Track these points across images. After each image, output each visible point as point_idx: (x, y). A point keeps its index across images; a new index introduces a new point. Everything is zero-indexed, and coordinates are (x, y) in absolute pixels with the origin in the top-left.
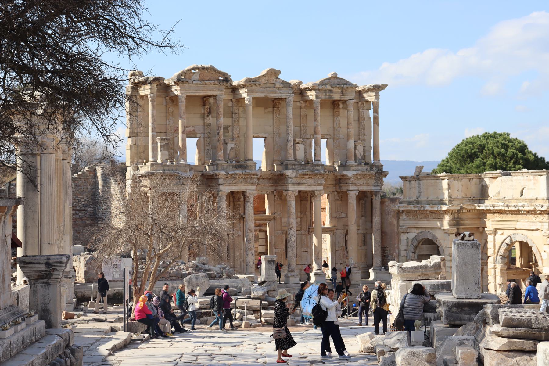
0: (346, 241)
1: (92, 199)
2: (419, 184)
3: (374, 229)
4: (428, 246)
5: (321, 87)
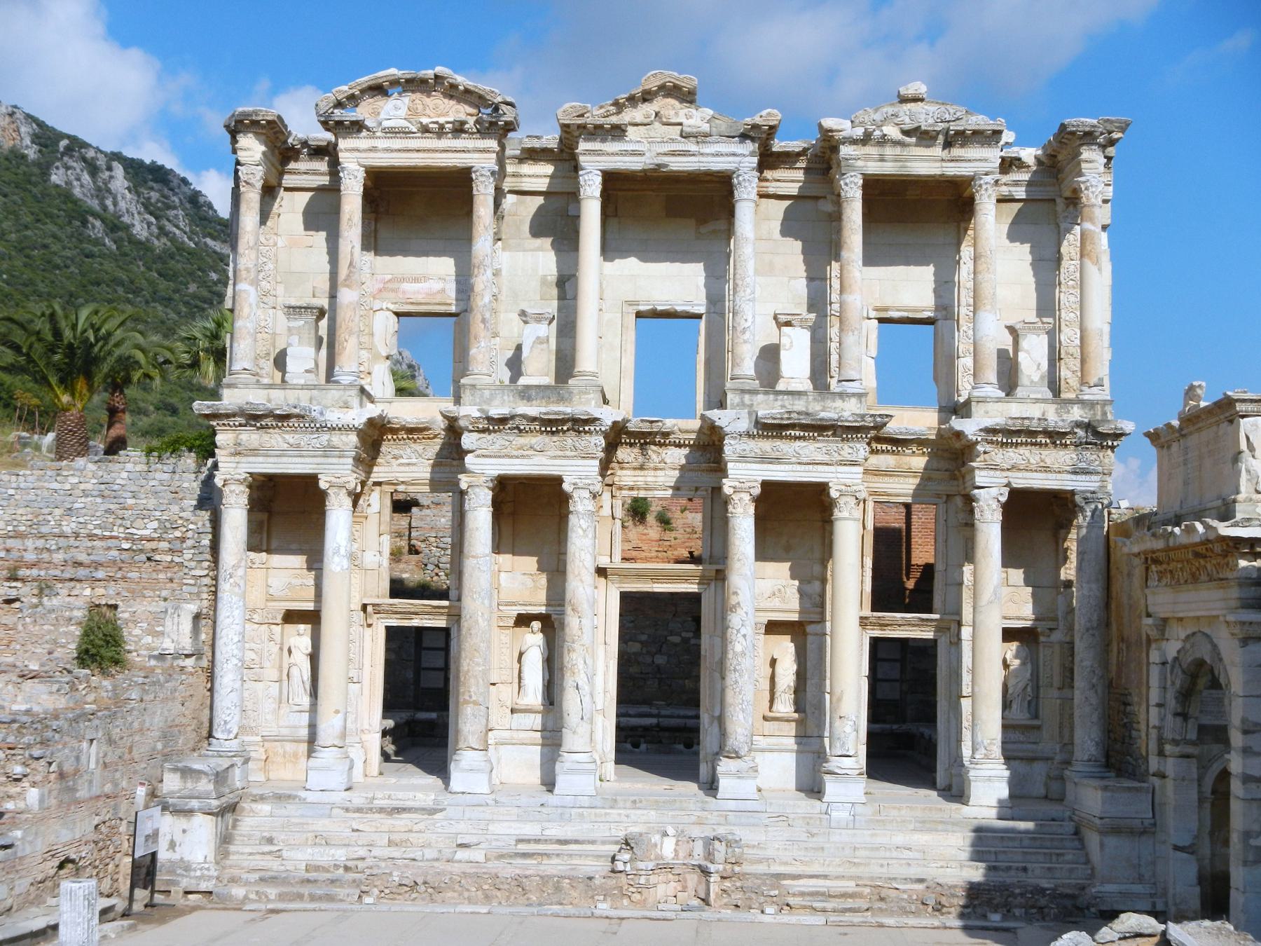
2: (1186, 450)
5: (859, 132)
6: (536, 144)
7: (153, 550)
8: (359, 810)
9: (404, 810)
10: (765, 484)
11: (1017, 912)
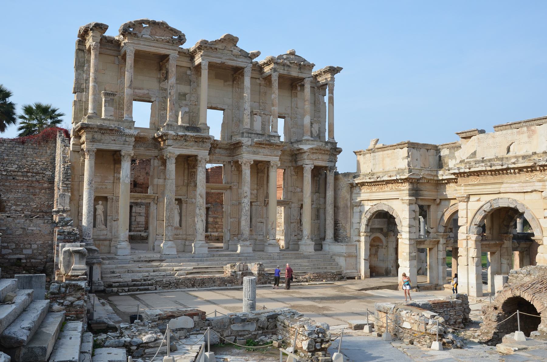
0: (301, 214)
1: (51, 163)
2: (375, 156)
3: (327, 203)
4: (379, 220)
5: (279, 61)
6: (181, 50)
7: (15, 175)
8: (138, 261)
9: (153, 261)
10: (254, 161)
11: (329, 279)
